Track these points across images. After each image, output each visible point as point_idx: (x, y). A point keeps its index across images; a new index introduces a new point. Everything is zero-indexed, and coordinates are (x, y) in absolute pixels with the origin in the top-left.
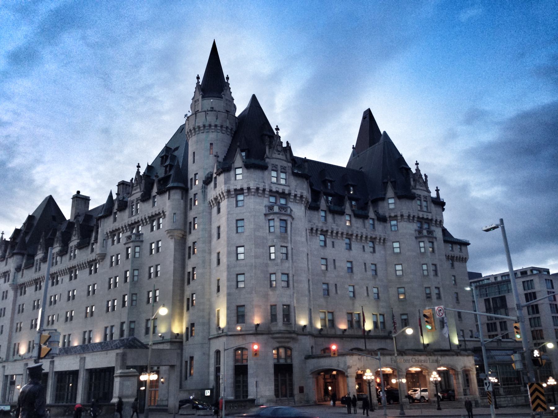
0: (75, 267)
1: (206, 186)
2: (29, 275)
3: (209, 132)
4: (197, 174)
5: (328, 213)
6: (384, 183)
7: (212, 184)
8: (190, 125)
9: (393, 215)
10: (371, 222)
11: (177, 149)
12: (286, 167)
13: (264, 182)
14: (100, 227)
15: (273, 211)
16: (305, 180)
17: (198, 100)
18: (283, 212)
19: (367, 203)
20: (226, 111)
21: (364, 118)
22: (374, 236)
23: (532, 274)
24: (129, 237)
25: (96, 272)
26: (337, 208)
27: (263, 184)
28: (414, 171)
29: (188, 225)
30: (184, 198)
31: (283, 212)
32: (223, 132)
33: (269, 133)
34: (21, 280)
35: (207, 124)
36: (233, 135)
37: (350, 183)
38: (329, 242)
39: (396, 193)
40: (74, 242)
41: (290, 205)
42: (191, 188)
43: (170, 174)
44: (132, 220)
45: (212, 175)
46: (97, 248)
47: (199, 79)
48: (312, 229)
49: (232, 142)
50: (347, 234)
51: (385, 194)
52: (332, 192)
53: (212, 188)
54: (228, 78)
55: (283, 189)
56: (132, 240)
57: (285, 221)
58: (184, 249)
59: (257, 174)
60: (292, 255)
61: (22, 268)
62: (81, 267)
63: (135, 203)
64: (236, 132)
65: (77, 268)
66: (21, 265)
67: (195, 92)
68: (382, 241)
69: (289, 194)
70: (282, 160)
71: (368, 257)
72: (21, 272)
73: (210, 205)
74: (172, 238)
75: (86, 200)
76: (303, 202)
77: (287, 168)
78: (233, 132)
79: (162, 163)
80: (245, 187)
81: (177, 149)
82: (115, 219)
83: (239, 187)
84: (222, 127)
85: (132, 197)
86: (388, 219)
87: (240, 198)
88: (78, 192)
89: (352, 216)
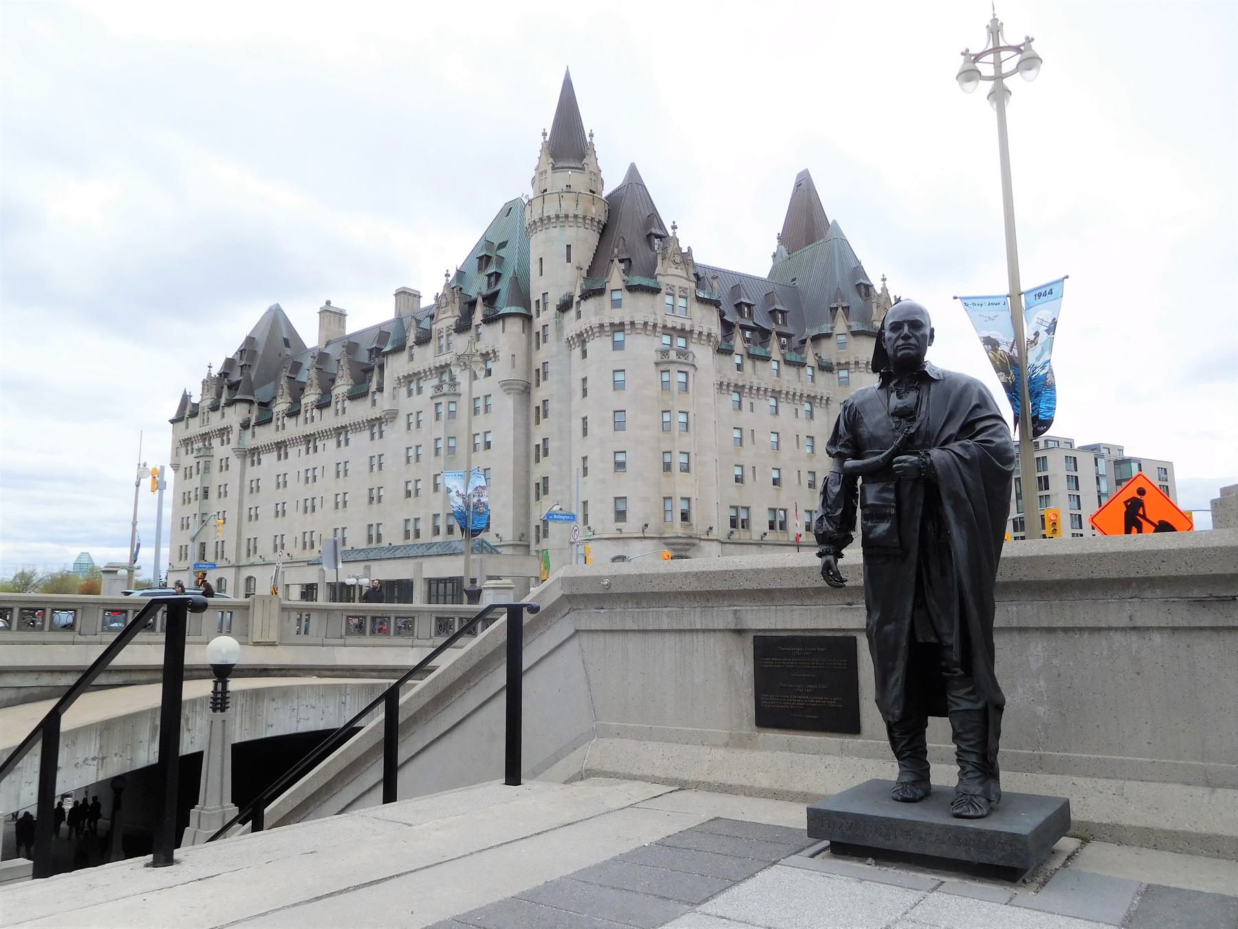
0: (345, 427)
1: (561, 314)
2: (266, 435)
3: (564, 226)
4: (547, 293)
5: (745, 357)
6: (831, 309)
7: (572, 313)
9: (843, 361)
10: (809, 371)
11: (503, 245)
12: (686, 289)
13: (655, 313)
14: (387, 367)
15: (668, 358)
16: (714, 309)
18: (682, 360)
19: (804, 342)
20: (591, 191)
21: (798, 185)
22: (813, 395)
23: (1047, 448)
24: (439, 388)
25: (381, 436)
26: (758, 351)
27: (654, 315)
28: (879, 291)
29: (534, 373)
30: (526, 331)
31: (682, 360)
32: (587, 226)
33: (659, 232)
34: (250, 442)
35: (562, 214)
36: (601, 232)
37: (778, 308)
38: (746, 403)
39: (849, 327)
40: (342, 387)
41: (692, 348)
42: (538, 316)
43: (497, 288)
44: (440, 361)
45: (572, 298)
46: (384, 402)
47: (546, 135)
48: (721, 383)
49: (599, 243)
50: (773, 391)
51: (832, 328)
52: (751, 324)
53: (572, 319)
54: (591, 135)
55: (682, 324)
56: (443, 392)
57: (686, 373)
58: (528, 410)
59: (644, 300)
60: (695, 425)
61: (252, 423)
62: (357, 427)
63: (444, 334)
64: (605, 226)
65: (349, 428)
66: (249, 420)
67: (539, 158)
68: (824, 402)
69: (691, 332)
70: (682, 277)
71: (803, 427)
72: (250, 431)
73: (568, 344)
74: (509, 394)
75: (341, 316)
76: (711, 344)
77: (689, 290)
78: (601, 227)
79: (480, 269)
80: (627, 320)
81: (503, 245)
82: (411, 358)
83: (617, 321)
84: (584, 218)
85: (438, 324)
86: (836, 367)
87: (619, 337)
88: (328, 303)
89: (782, 362)
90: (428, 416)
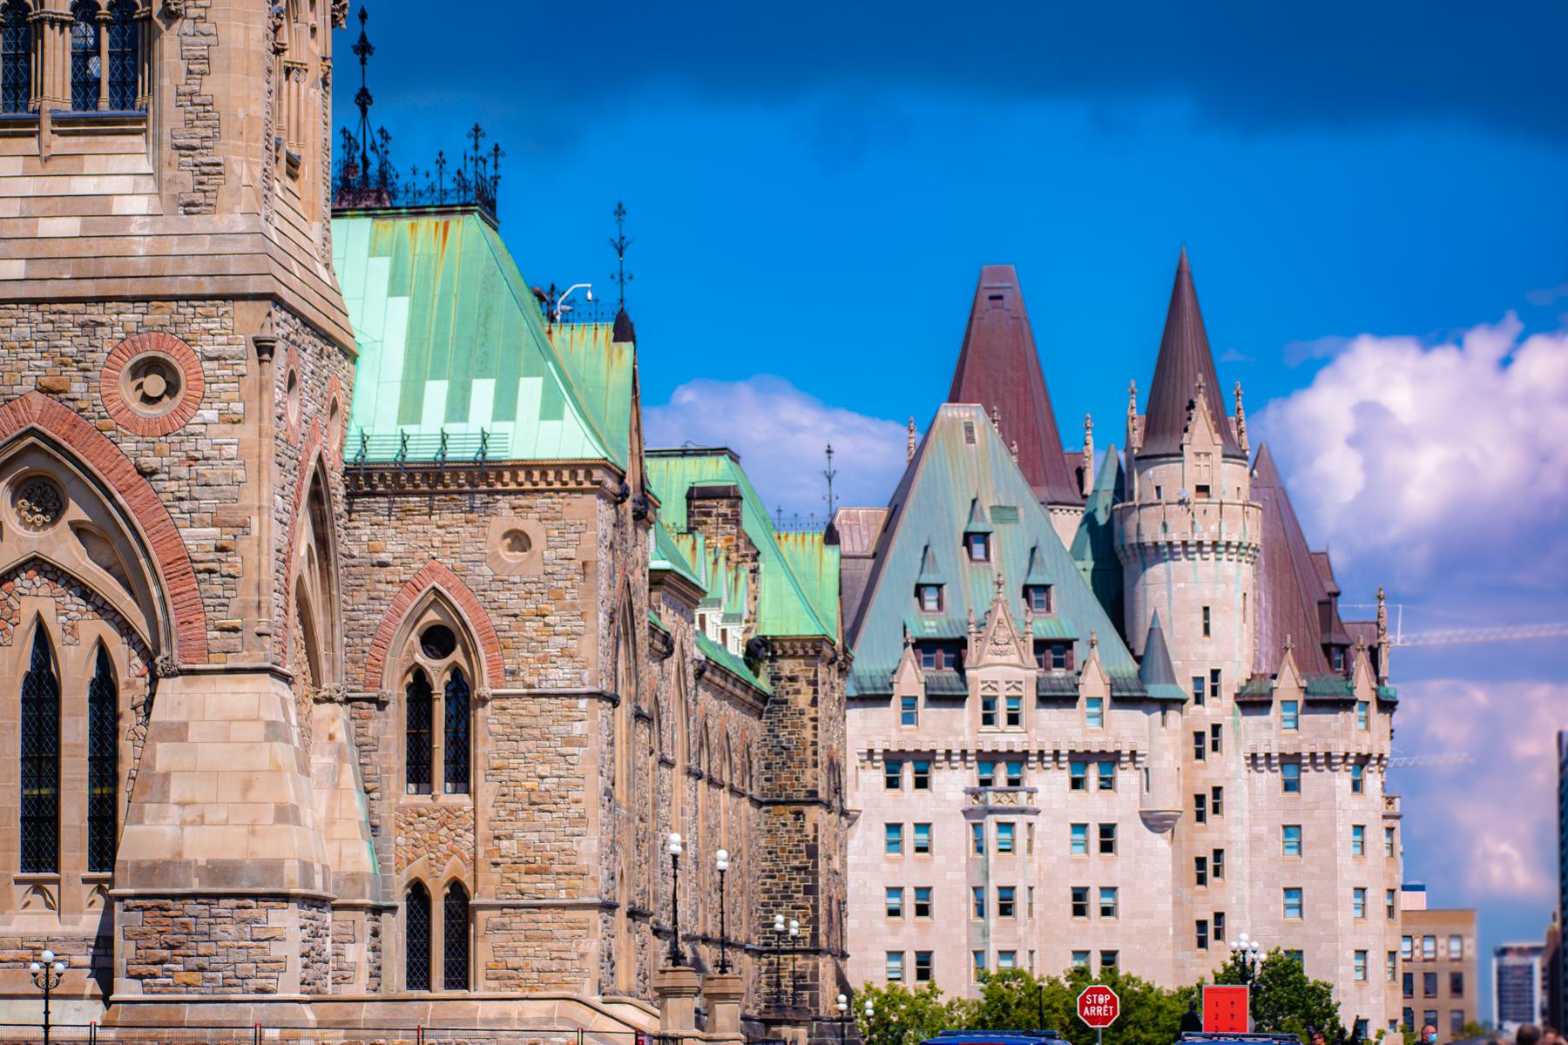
8: (1199, 527)
17: (1207, 454)
42: (1199, 699)
83: (1365, 752)
90: (953, 836)
